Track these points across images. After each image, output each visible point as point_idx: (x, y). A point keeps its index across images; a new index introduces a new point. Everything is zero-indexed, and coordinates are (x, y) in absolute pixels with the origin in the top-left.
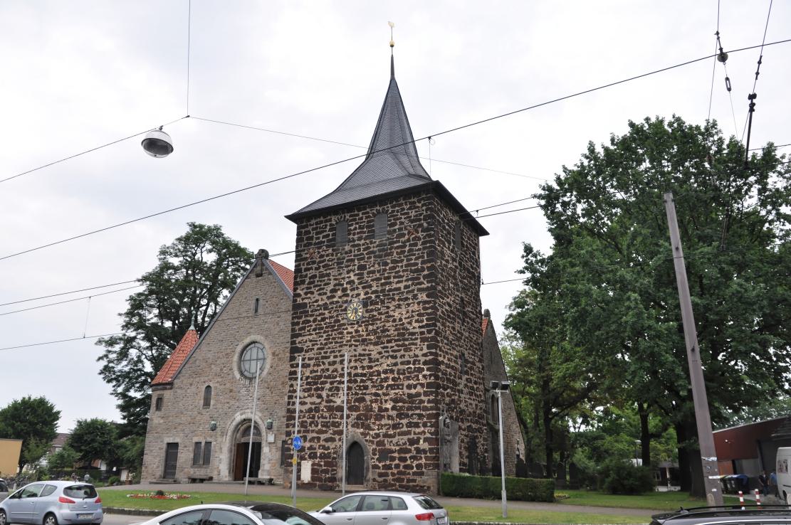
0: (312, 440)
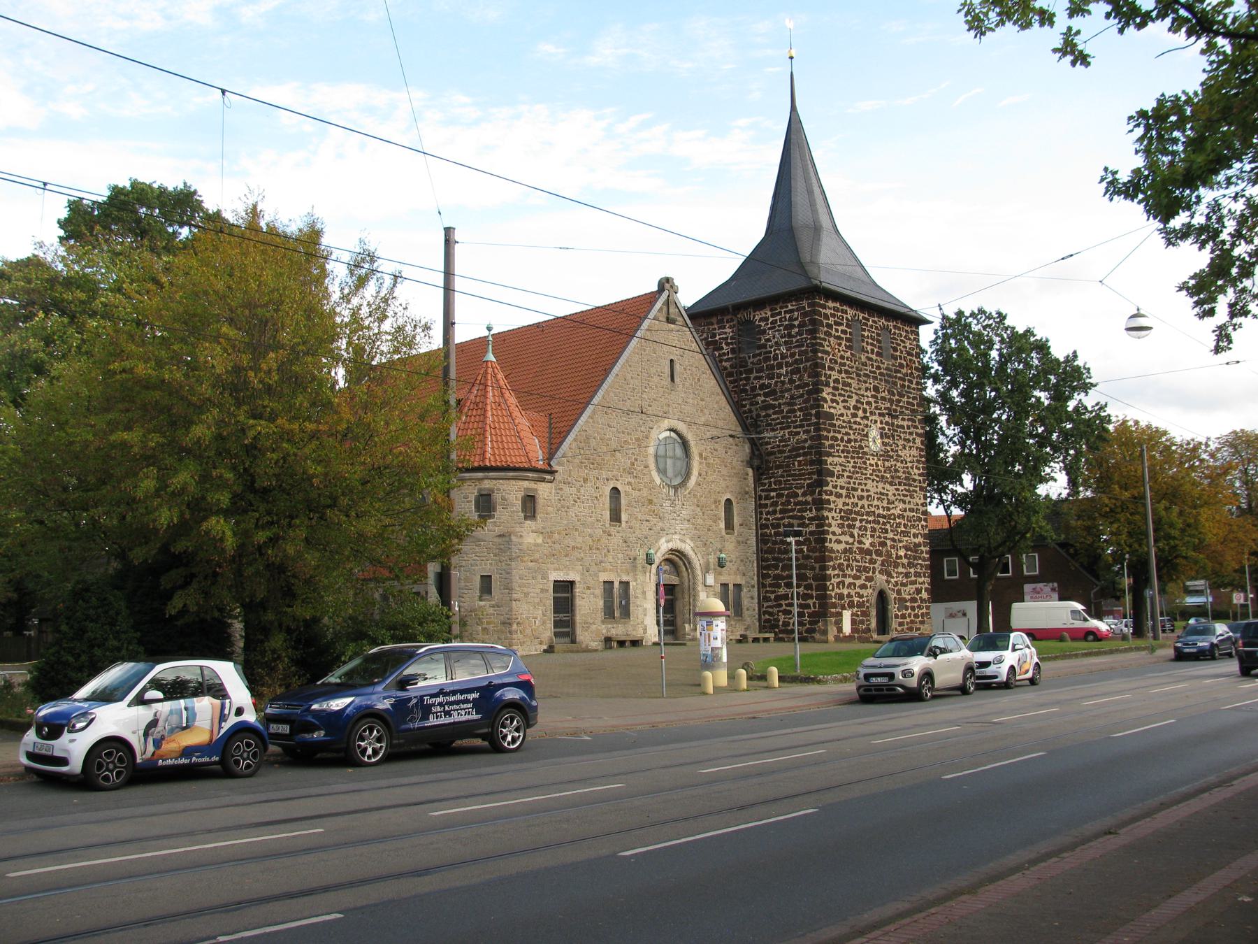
0: (850, 584)
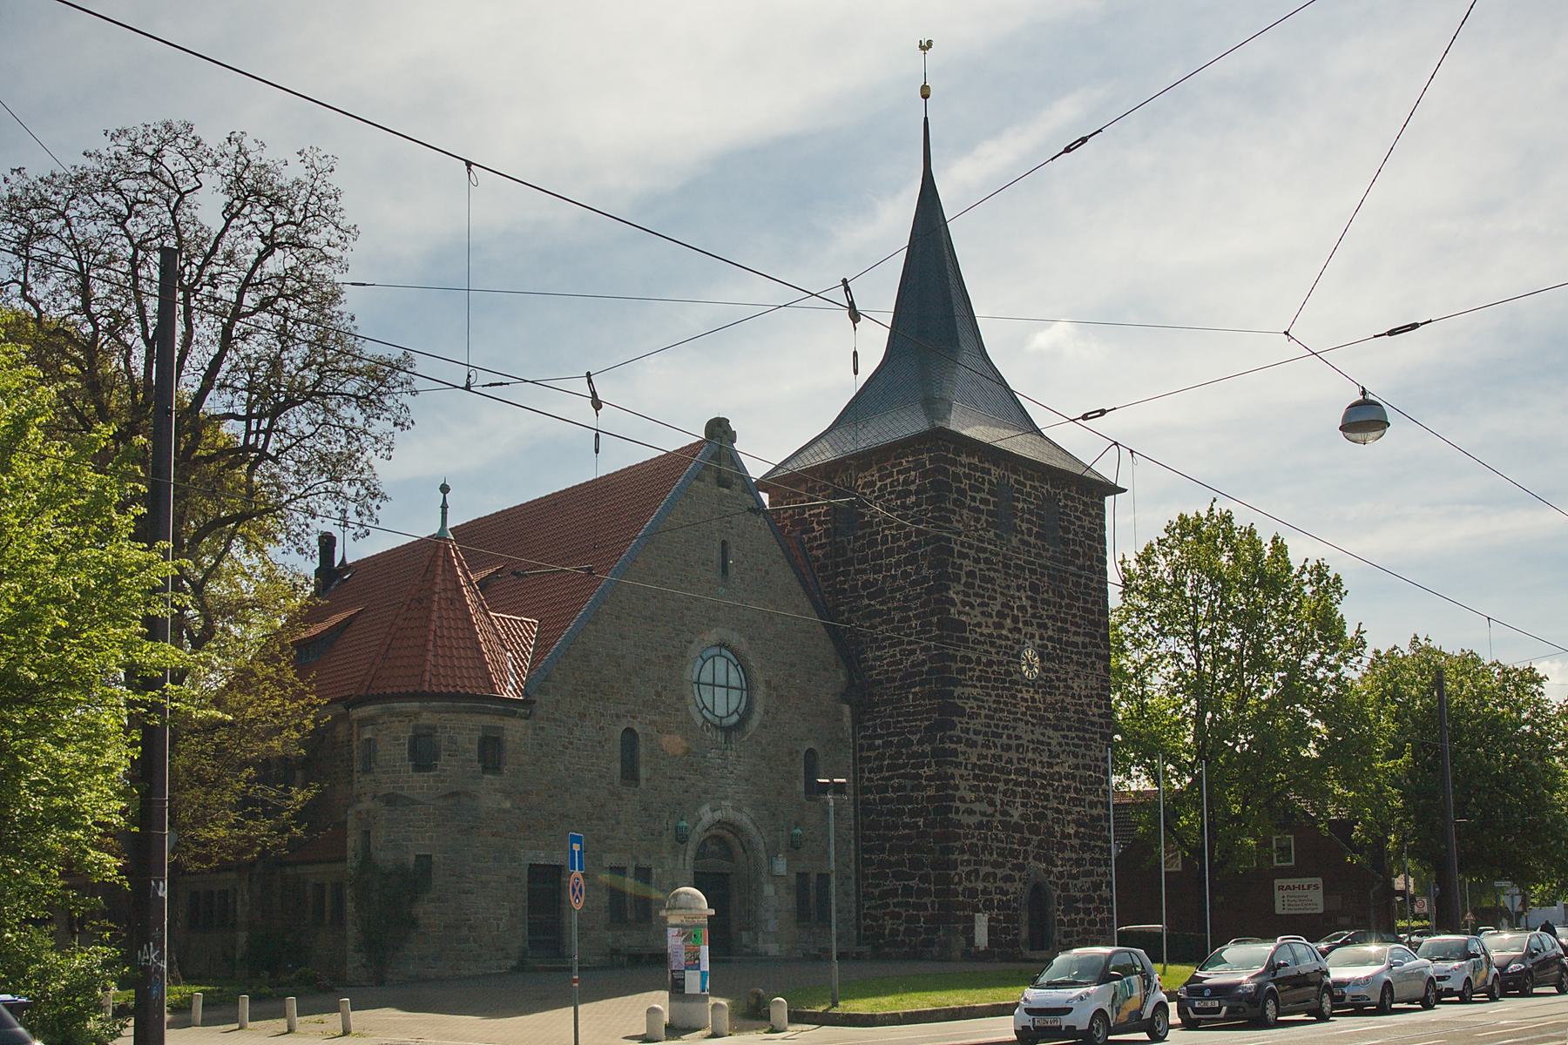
0: (987, 876)
